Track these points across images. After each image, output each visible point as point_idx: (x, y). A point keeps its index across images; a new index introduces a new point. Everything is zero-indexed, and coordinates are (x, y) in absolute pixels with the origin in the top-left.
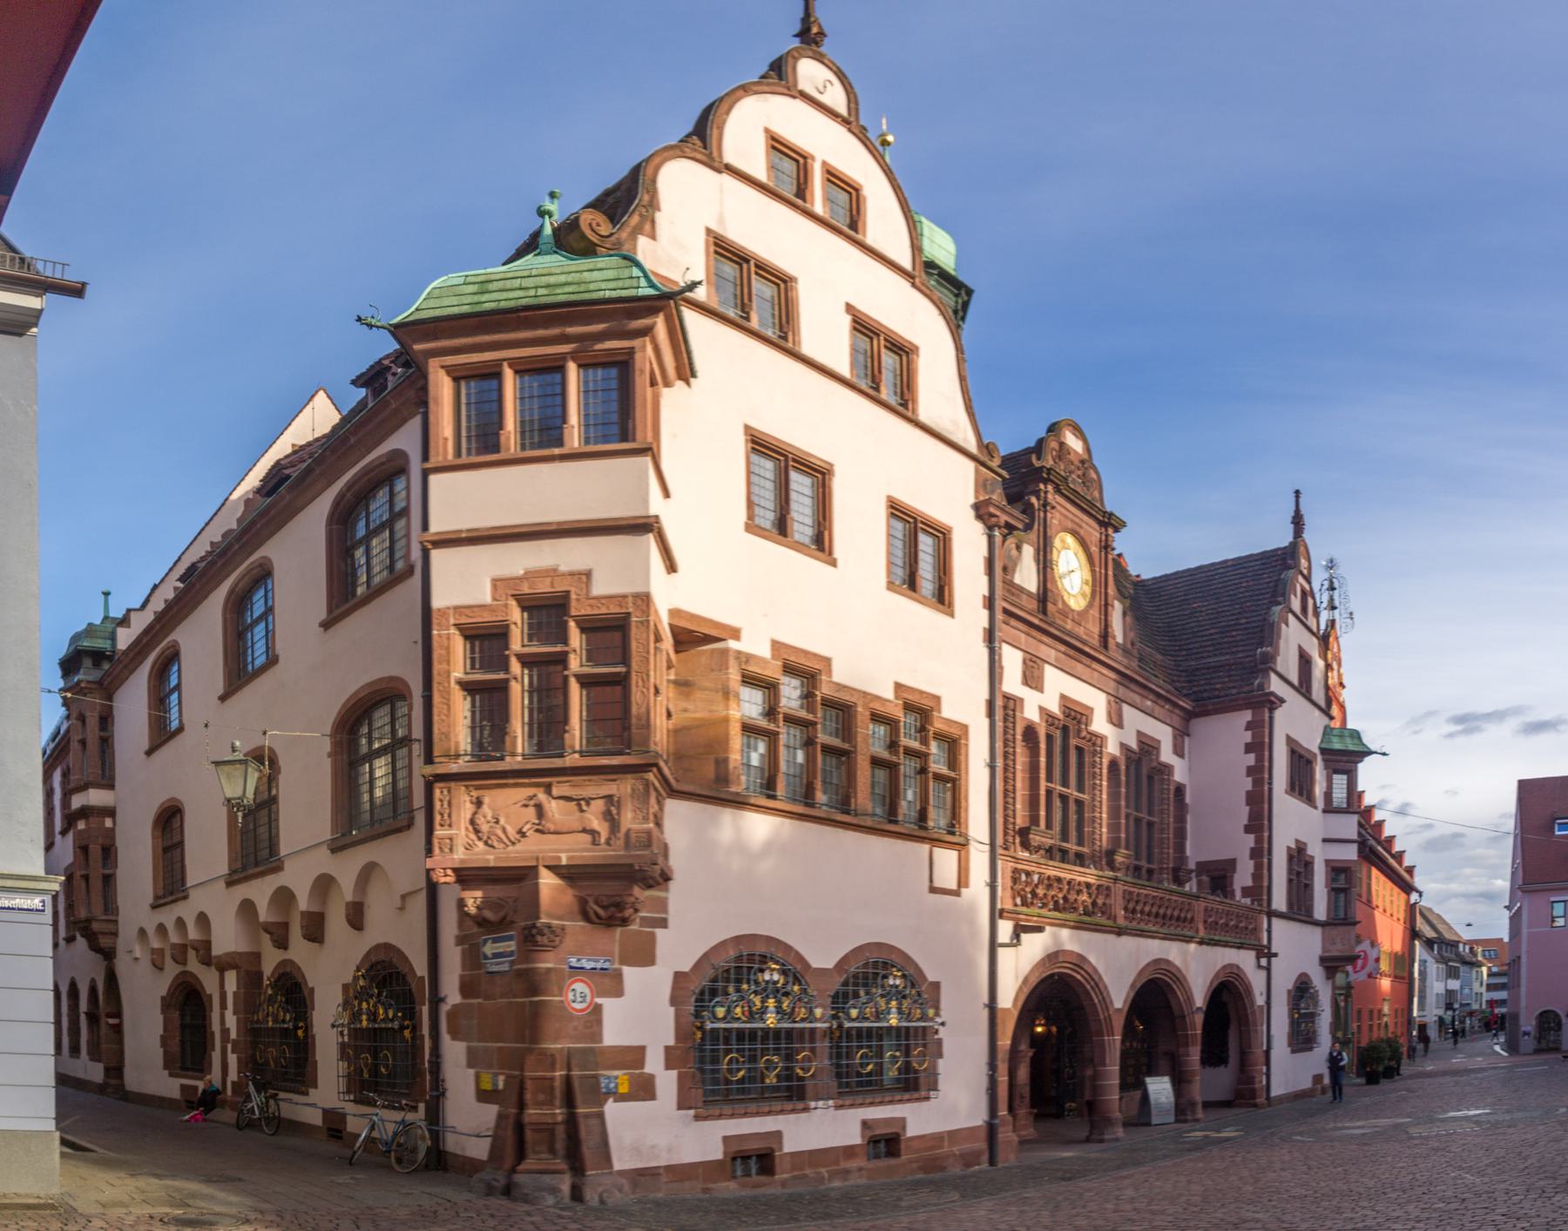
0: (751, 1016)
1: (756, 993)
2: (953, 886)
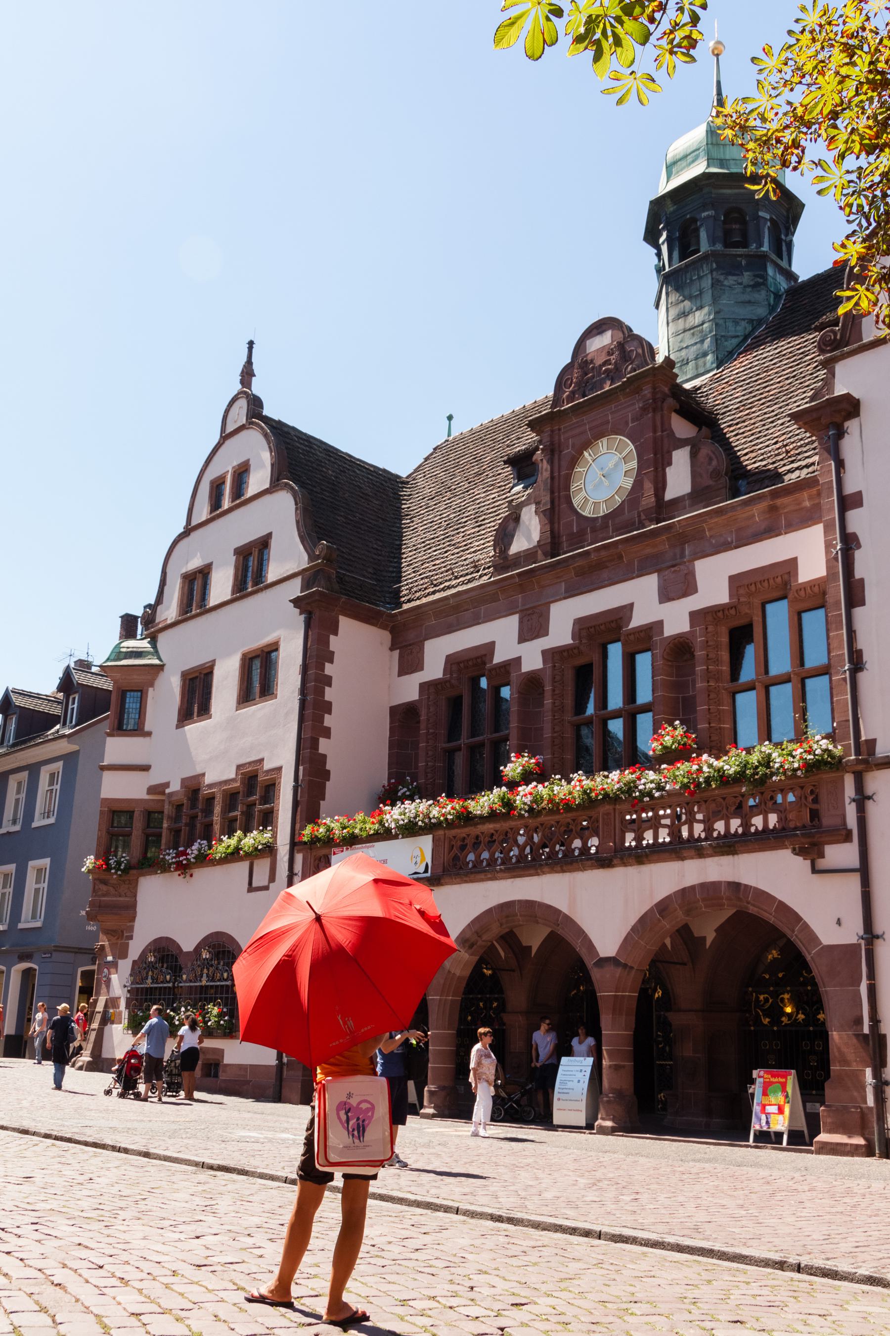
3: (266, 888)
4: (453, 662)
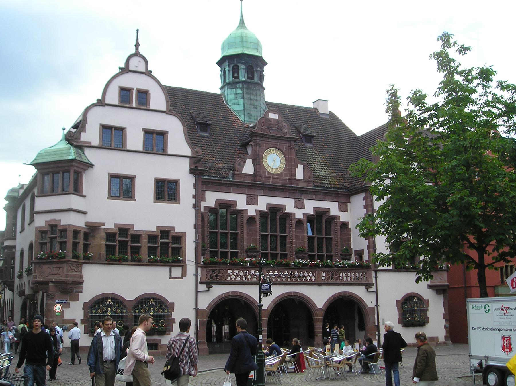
0: (103, 312)
1: (104, 307)
3: (182, 278)
4: (218, 202)
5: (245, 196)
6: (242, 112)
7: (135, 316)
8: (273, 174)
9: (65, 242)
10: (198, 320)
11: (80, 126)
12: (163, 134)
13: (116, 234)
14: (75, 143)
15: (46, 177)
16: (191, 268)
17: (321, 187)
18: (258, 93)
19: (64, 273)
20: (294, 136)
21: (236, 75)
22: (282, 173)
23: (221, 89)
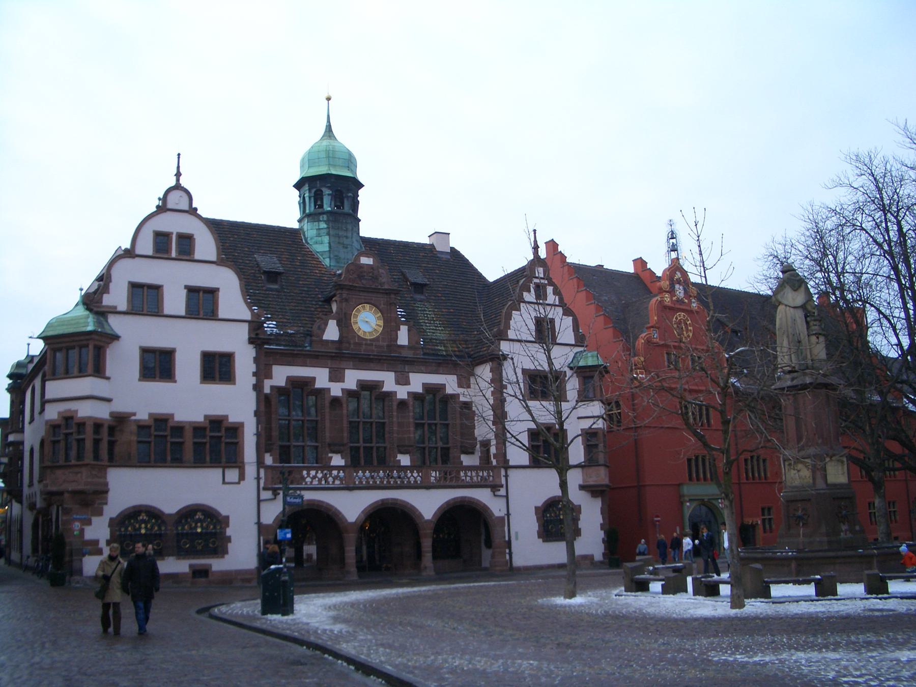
2: (237, 480)
3: (239, 483)
5: (327, 370)
6: (327, 254)
7: (178, 534)
8: (366, 340)
9: (83, 440)
10: (262, 538)
11: (104, 279)
12: (212, 292)
13: (149, 427)
14: (95, 309)
15: (58, 355)
16: (251, 470)
17: (434, 354)
18: (349, 227)
19: (81, 480)
20: (395, 286)
21: (319, 203)
22: (378, 337)
23: (300, 221)
